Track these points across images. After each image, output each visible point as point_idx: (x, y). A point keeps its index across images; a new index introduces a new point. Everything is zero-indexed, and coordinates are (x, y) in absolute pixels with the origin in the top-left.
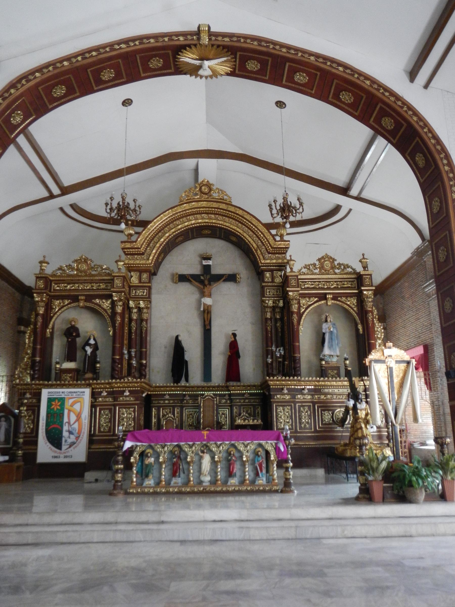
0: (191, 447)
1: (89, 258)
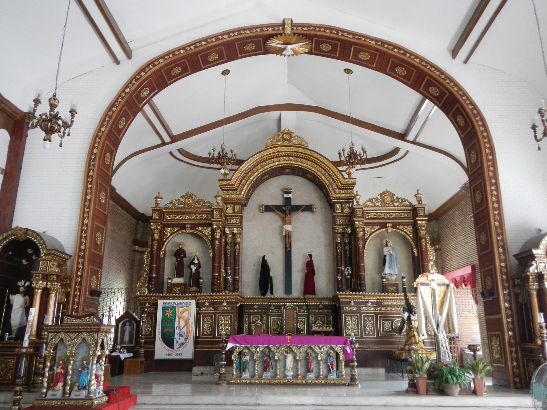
0: (278, 348)
1: (194, 194)
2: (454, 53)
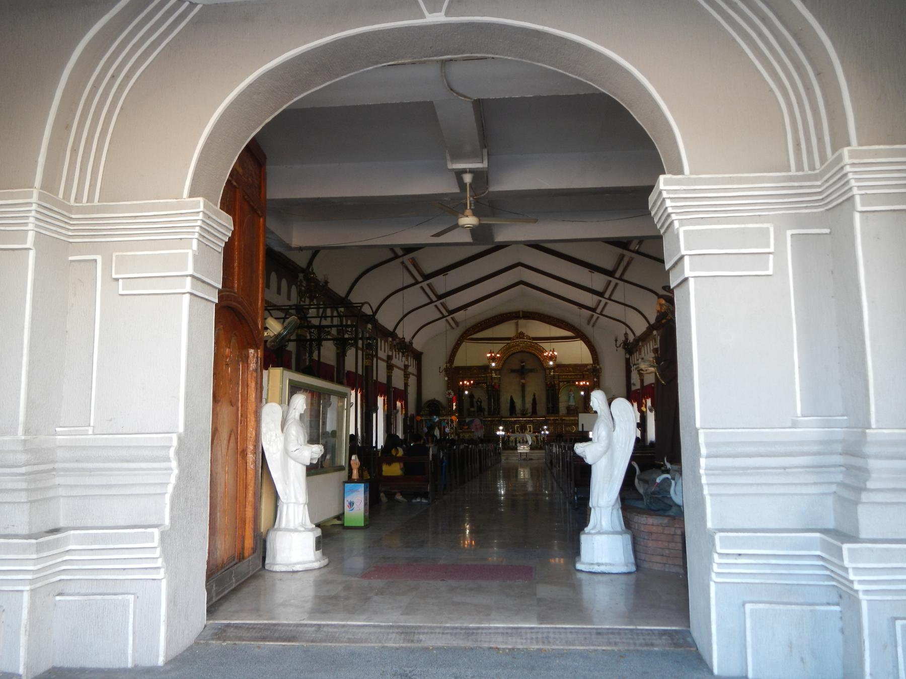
2: (589, 323)
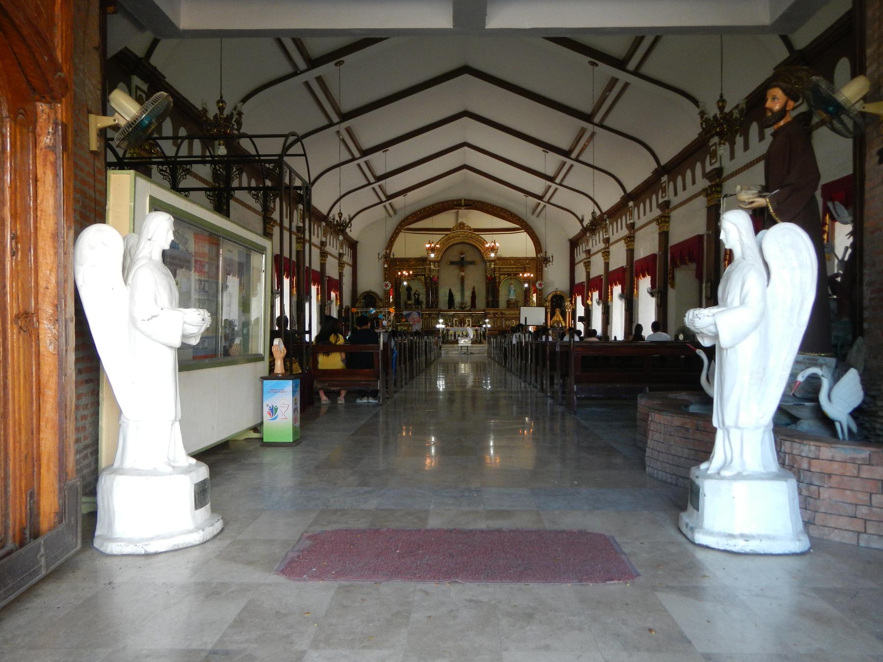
2: (533, 213)
